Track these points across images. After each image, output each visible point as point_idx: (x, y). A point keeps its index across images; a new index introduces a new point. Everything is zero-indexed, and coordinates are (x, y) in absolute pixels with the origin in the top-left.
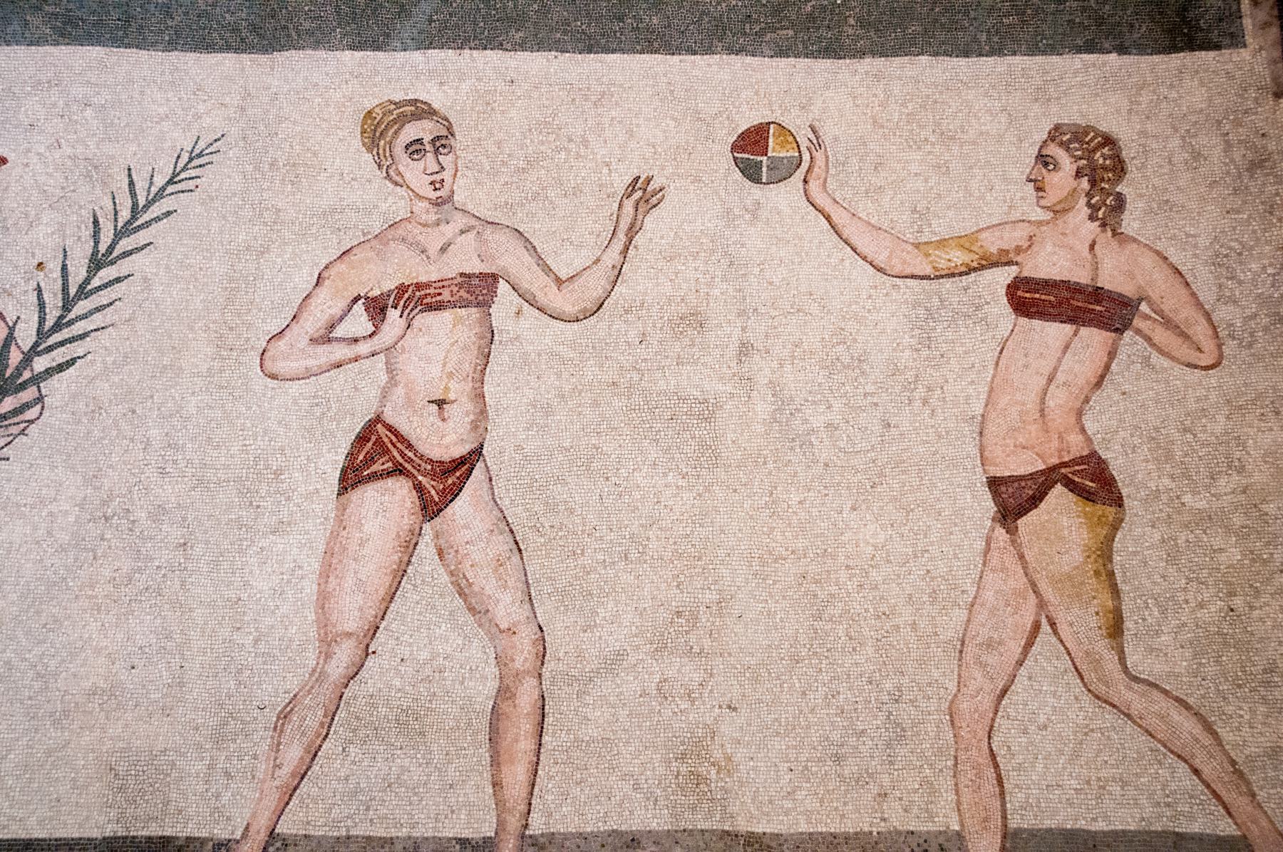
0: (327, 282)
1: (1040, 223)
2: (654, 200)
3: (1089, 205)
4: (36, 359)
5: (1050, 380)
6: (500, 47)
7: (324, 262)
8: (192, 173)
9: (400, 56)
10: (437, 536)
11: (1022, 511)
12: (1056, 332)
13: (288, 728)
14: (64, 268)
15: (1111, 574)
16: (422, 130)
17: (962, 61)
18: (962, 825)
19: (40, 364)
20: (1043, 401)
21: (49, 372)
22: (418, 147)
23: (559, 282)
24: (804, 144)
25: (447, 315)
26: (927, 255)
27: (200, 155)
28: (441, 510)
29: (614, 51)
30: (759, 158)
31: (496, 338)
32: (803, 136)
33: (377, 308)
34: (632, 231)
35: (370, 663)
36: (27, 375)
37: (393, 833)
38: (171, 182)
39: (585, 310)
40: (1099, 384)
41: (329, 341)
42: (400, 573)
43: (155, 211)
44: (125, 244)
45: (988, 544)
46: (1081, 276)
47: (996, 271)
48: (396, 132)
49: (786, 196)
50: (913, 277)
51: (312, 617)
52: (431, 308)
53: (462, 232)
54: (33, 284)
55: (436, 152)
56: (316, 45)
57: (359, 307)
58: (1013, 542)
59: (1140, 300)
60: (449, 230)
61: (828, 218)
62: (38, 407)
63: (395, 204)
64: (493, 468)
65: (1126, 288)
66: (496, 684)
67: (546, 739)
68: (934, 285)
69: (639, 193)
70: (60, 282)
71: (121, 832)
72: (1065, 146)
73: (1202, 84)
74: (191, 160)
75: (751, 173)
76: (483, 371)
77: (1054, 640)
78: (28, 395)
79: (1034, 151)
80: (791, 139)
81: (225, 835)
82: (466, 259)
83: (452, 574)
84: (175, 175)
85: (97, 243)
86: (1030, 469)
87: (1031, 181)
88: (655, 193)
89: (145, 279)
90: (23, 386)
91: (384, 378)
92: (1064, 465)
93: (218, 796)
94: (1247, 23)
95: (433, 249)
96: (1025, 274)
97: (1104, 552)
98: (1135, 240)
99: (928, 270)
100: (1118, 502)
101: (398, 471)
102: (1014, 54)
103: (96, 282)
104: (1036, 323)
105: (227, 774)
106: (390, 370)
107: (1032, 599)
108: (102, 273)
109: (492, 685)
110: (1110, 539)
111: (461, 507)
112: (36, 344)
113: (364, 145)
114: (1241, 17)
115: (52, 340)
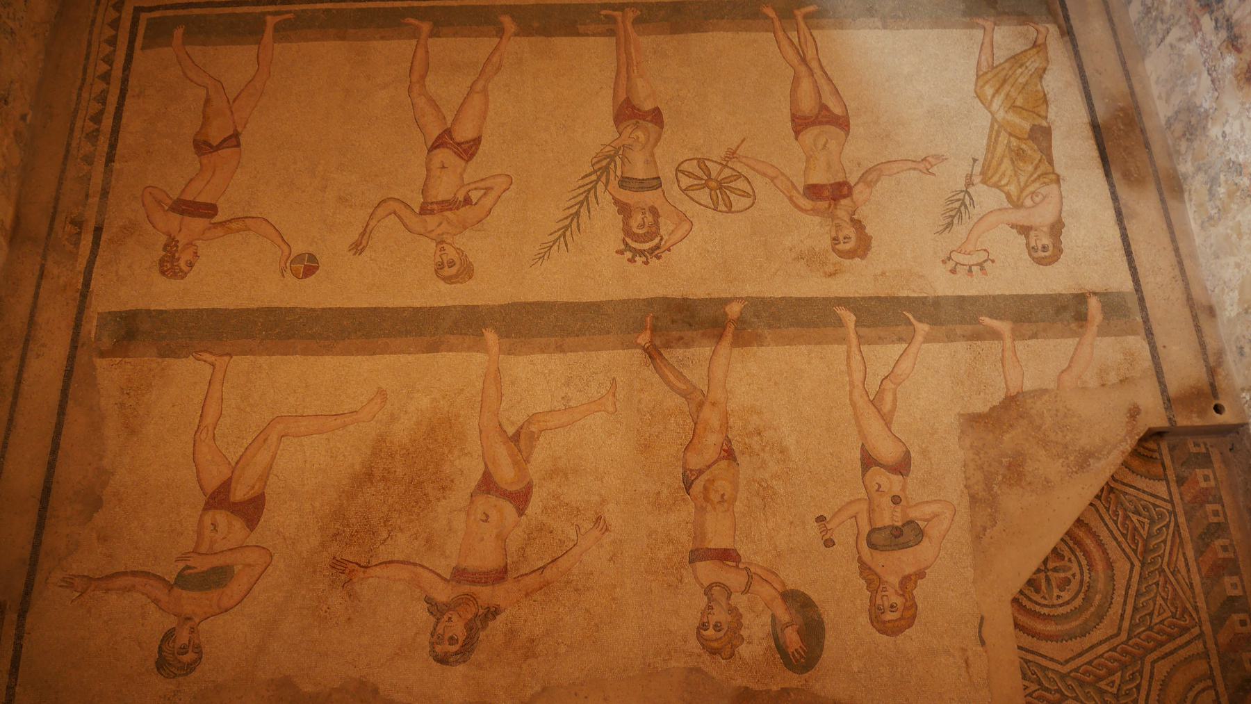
0: (487, 210)
1: (198, 239)
2: (354, 246)
3: (177, 247)
4: (596, 179)
5: (209, 181)
6: (414, 308)
7: (488, 218)
8: (542, 251)
9: (457, 303)
10: (446, 123)
11: (230, 137)
12: (202, 199)
13: (497, 66)
14: (589, 212)
15: (204, 117)
16: (448, 272)
17: (216, 306)
18: (273, 45)
19: (594, 177)
20: (214, 173)
21: (590, 174)
22: (452, 264)
23: (395, 213)
24: (289, 268)
25: (440, 199)
26: (246, 226)
27: (540, 258)
28: (444, 131)
29: (365, 308)
30: (308, 264)
31: (421, 191)
32: (288, 273)
33: (467, 201)
34: (363, 234)
35: (470, 85)
36: (598, 173)
37: (462, 39)
38: (551, 247)
39: (385, 202)
40: (191, 180)
41: (486, 189)
42: (459, 111)
43: (556, 235)
44: (567, 222)
45: (245, 125)
46: (188, 219)
47: (220, 221)
48: (459, 271)
49: (299, 248)
50: (253, 218)
51: (490, 98)
52: (447, 201)
53: (433, 231)
54: (600, 205)
55: (443, 263)
56: (493, 308)
57: (474, 201)
58: (236, 127)
59: (167, 210)
60: (439, 231)
61: (283, 240)
62: (593, 162)
63: (462, 241)
64: (425, 146)
65: (171, 214)
66: (426, 80)
67: (410, 65)
68: (245, 215)
69: (361, 247)
70: (590, 207)
71: (549, 38)
72: (181, 270)
73: (120, 297)
74: (543, 256)
75: (312, 257)
76: (426, 179)
77: (229, 97)
78: (596, 167)
79: (194, 268)
80: (294, 272)
81: (518, 38)
82: (432, 221)
83: (440, 112)
84: (550, 250)
85: (578, 222)
86: (224, 150)
87: (199, 256)
88: (352, 249)
89: (558, 209)
90: (599, 169)
91: (464, 176)
92: (211, 152)
93: (519, 47)
94: (95, 323)
95: (445, 224)
96: (209, 220)
97: (203, 125)
98: (163, 233)
99: (246, 220)
100: (194, 141)
101: (459, 144)
102: (193, 310)
103: (577, 207)
104: (209, 201)
105: (517, 53)
106: (462, 179)
107: (233, 109)
108: (575, 211)
109: (427, 79)
110: (201, 129)
111: (436, 133)
112: (597, 184)
113: (472, 265)
114: (97, 326)
115: (592, 185)
